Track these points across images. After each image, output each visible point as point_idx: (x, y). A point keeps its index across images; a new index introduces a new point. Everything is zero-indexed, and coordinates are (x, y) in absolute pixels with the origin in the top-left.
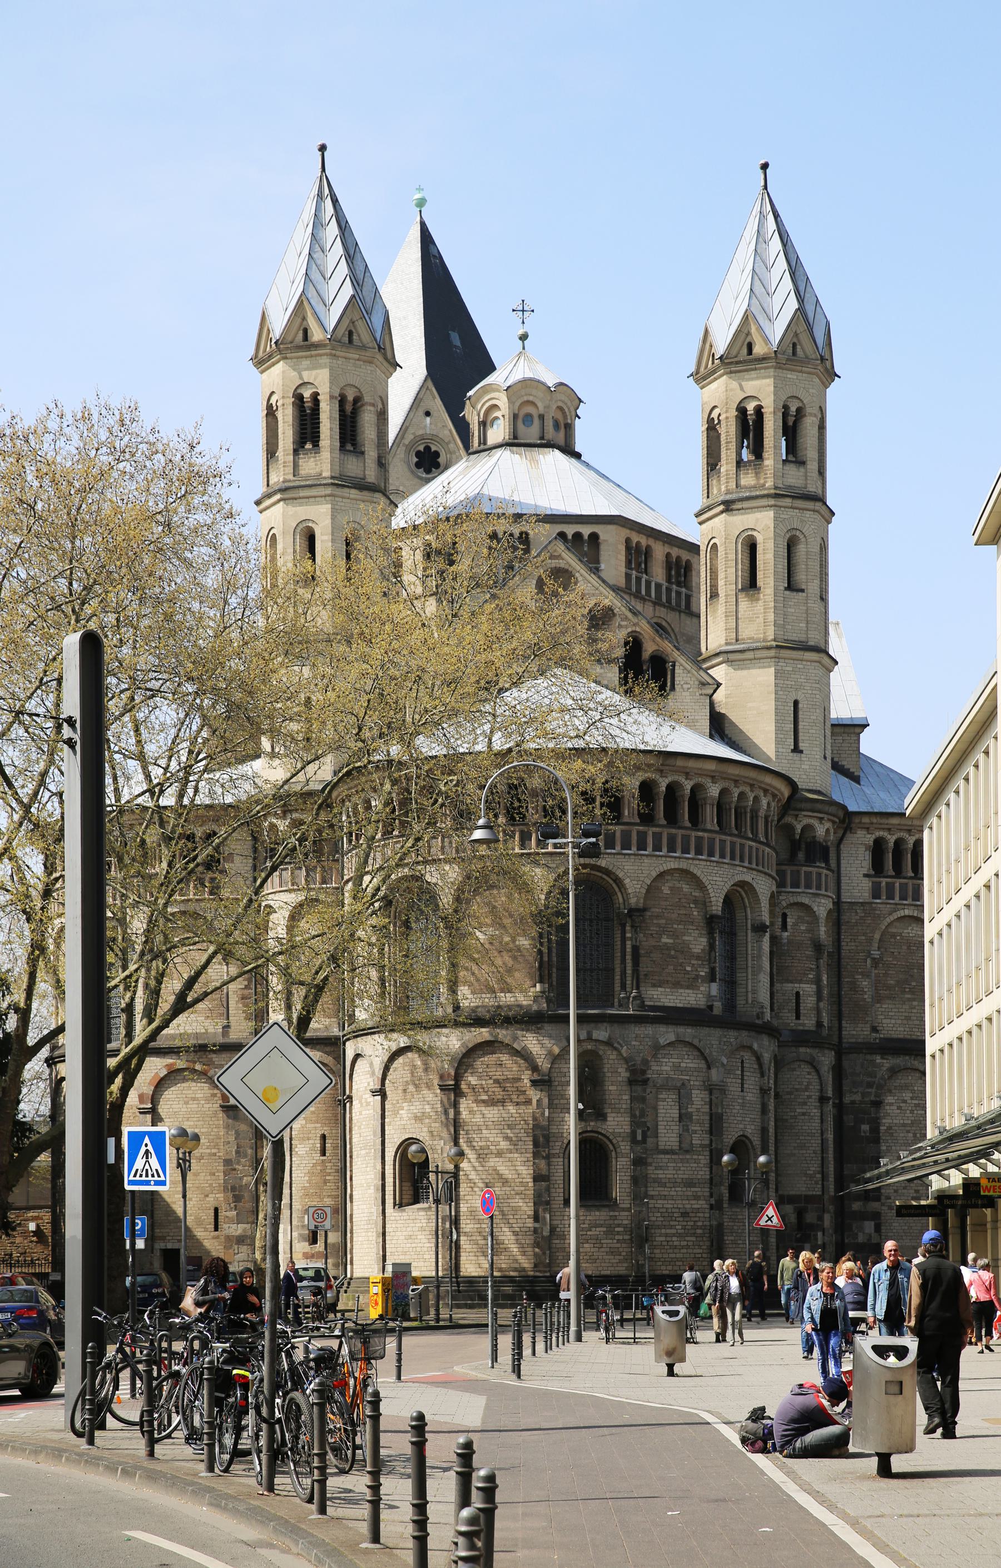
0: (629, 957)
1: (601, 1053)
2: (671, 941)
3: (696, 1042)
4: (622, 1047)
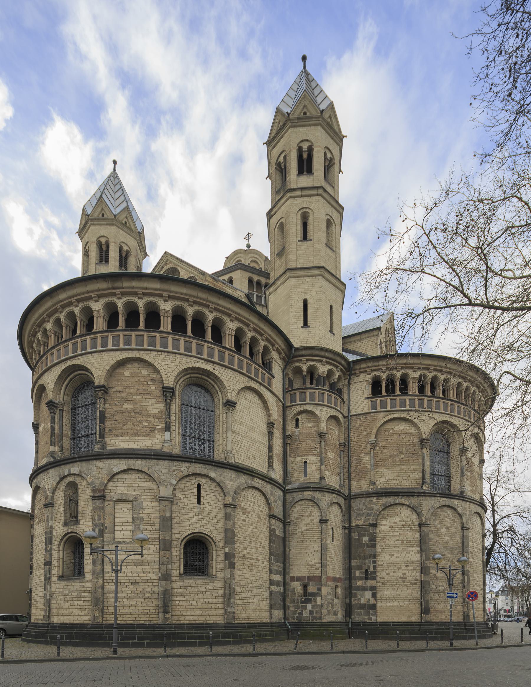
1: (77, 482)
2: (131, 407)
3: (145, 469)
4: (87, 476)
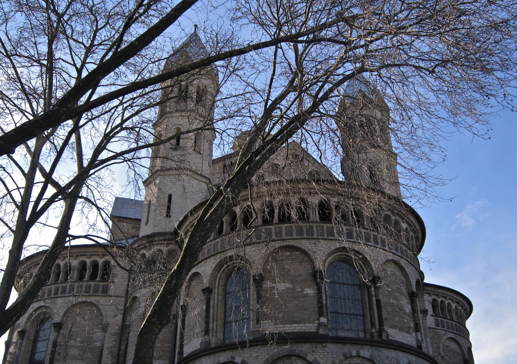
0: (375, 307)
